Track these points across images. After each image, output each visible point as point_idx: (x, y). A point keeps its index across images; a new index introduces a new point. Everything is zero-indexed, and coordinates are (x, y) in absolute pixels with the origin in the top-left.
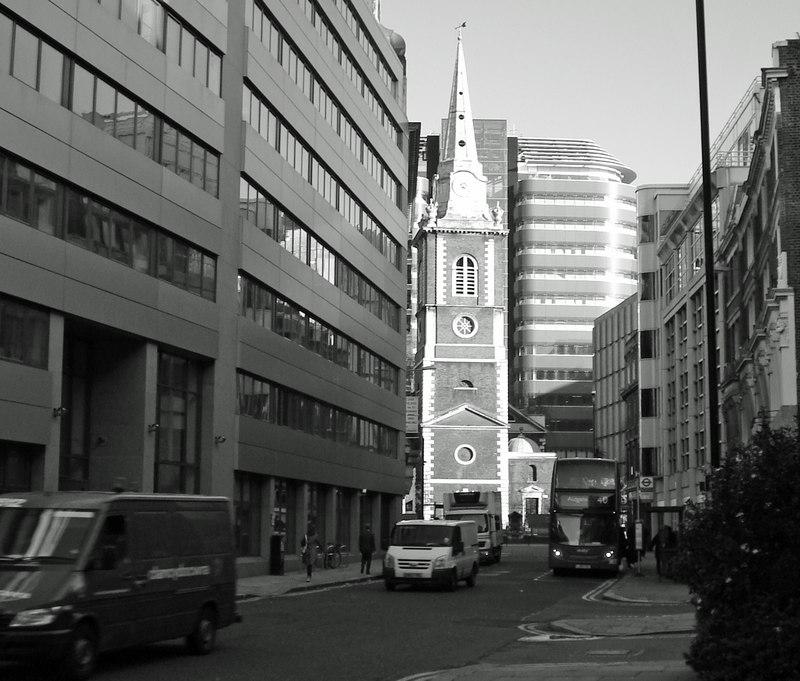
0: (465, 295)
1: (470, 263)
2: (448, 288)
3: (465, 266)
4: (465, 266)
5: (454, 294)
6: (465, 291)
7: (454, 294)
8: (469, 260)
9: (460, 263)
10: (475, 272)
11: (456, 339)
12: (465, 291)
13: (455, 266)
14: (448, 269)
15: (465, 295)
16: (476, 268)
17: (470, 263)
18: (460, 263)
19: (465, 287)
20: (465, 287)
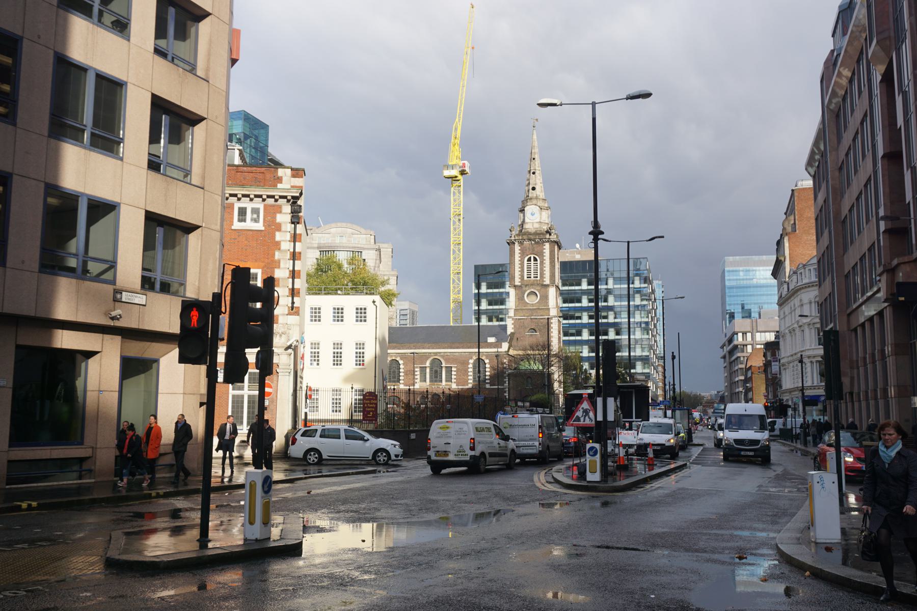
1: (535, 259)
7: (525, 278)
9: (529, 260)
17: (535, 259)
18: (529, 260)
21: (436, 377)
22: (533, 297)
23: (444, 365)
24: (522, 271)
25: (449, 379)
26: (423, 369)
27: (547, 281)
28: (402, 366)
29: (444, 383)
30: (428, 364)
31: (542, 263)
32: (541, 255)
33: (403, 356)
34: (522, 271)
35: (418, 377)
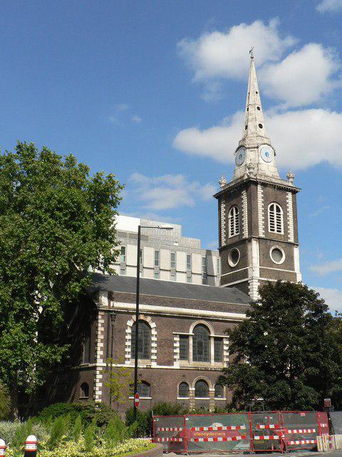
0: (275, 232)
1: (278, 210)
5: (269, 231)
6: (276, 229)
7: (269, 231)
8: (277, 207)
9: (272, 208)
10: (282, 217)
11: (272, 264)
12: (276, 229)
13: (269, 211)
14: (265, 211)
15: (275, 232)
16: (282, 213)
17: (278, 210)
18: (272, 208)
19: (276, 226)
20: (276, 226)
21: (200, 353)
22: (277, 255)
23: (212, 335)
24: (266, 220)
25: (218, 358)
26: (184, 338)
28: (154, 332)
29: (213, 361)
30: (191, 333)
31: (286, 216)
33: (156, 315)
35: (177, 351)
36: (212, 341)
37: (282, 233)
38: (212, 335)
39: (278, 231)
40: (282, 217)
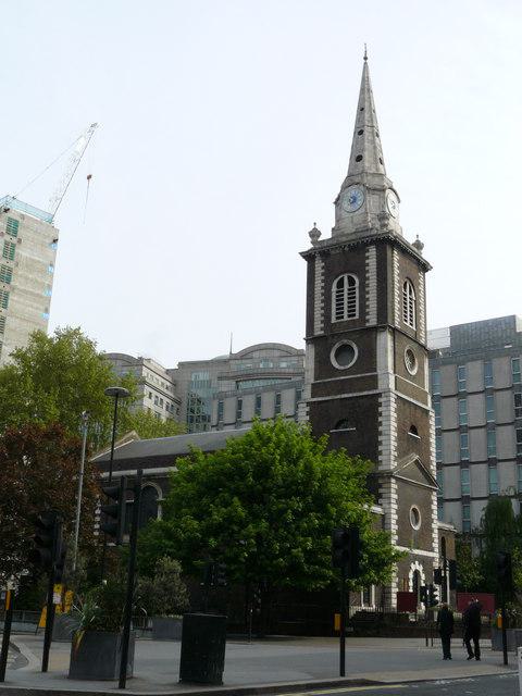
1: (351, 282)
2: (327, 316)
3: (346, 286)
4: (346, 286)
6: (346, 314)
7: (334, 320)
8: (349, 277)
9: (340, 284)
10: (357, 291)
11: (335, 372)
12: (346, 314)
13: (334, 289)
15: (346, 318)
16: (357, 280)
17: (351, 282)
18: (340, 284)
24: (327, 308)
27: (372, 321)
31: (363, 286)
32: (361, 270)
34: (327, 308)
36: (160, 507)
37: (357, 317)
38: (161, 499)
39: (349, 316)
40: (357, 291)
